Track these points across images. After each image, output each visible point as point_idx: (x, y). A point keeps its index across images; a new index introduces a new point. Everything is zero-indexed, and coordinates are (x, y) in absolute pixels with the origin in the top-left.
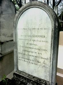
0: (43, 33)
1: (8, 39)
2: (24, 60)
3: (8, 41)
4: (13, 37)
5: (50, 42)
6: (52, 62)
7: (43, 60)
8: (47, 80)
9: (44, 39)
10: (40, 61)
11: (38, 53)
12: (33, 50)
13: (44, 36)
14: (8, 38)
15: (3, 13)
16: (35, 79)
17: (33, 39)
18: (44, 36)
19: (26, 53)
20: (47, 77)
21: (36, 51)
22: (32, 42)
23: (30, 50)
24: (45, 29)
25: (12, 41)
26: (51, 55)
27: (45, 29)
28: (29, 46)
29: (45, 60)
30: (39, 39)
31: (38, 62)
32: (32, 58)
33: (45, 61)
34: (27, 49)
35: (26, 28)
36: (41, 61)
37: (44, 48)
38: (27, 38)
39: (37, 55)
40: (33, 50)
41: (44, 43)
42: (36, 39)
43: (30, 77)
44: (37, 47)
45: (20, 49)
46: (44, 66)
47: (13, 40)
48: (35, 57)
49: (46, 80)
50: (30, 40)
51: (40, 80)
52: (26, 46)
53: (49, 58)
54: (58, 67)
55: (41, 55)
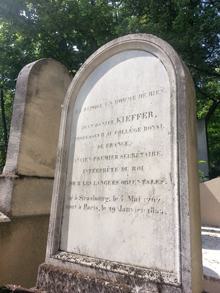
0: (147, 104)
1: (41, 171)
2: (85, 205)
3: (39, 178)
4: (54, 168)
5: (169, 126)
6: (176, 187)
7: (149, 187)
8: (163, 268)
9: (148, 122)
10: (137, 196)
11: (134, 168)
12: (116, 163)
13: (151, 114)
14: (42, 166)
15: (41, 95)
16: (122, 271)
17: (118, 127)
18: (151, 114)
19: (95, 177)
20: (166, 251)
21: (127, 162)
22: (114, 139)
23: (106, 164)
24: (151, 94)
25: (49, 181)
26: (172, 163)
27: (151, 94)
28: (105, 152)
29: (155, 186)
30: (136, 123)
31: (132, 199)
32: (110, 191)
33: (154, 190)
34: (96, 165)
35: (98, 103)
36: (142, 191)
37: (150, 149)
38: (100, 130)
39: (129, 175)
40: (116, 163)
41: (150, 134)
42: (126, 126)
43: (101, 266)
44: (128, 150)
45: (78, 171)
46: (152, 210)
47: (53, 178)
48: (124, 182)
49: (159, 265)
50: (109, 134)
51: (138, 272)
52: (95, 155)
53: (168, 177)
54: (204, 264)
55: (140, 171)
